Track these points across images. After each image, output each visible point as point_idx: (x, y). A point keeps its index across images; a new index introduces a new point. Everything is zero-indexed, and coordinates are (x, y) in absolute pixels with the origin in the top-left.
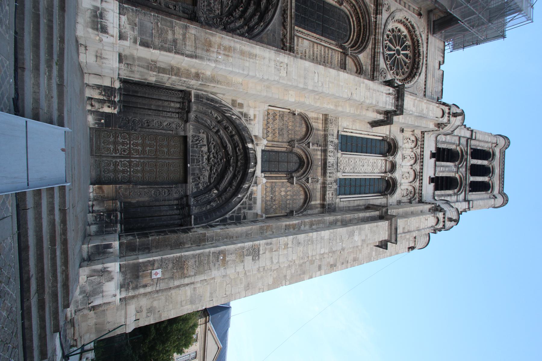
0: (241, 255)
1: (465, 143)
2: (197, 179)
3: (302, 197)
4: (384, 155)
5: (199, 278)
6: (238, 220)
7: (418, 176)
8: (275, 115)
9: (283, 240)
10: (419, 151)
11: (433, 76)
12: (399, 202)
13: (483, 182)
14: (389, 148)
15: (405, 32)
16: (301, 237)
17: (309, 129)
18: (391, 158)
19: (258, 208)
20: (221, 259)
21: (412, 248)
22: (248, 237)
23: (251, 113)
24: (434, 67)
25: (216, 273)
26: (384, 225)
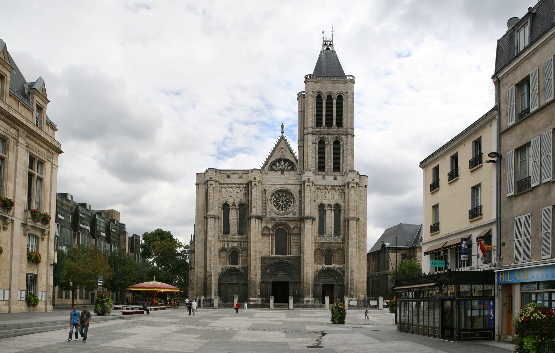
0: (352, 275)
1: (315, 136)
2: (333, 282)
3: (339, 251)
4: (325, 210)
5: (355, 284)
6: (344, 272)
7: (333, 187)
8: (315, 261)
9: (350, 264)
10: (322, 187)
11: (288, 179)
12: (344, 202)
13: (337, 103)
14: (322, 208)
15: (273, 197)
16: (350, 258)
17: (318, 249)
18: (326, 208)
19: (342, 266)
20: (352, 280)
21: (366, 187)
22: (348, 272)
23: (316, 269)
24: (285, 178)
25: (355, 281)
26: (350, 222)
